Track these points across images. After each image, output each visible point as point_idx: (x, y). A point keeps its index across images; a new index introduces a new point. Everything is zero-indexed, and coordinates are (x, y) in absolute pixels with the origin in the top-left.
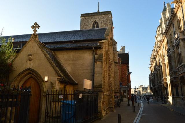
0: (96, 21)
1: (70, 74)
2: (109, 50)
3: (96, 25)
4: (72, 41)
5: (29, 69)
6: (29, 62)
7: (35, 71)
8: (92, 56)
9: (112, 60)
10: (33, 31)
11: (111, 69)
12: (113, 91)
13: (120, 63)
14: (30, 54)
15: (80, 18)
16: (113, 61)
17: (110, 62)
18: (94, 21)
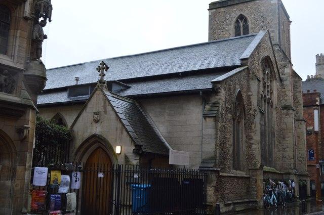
0: (241, 15)
1: (164, 140)
2: (249, 88)
3: (241, 24)
4: (179, 73)
5: (94, 136)
6: (95, 125)
7: (105, 139)
8: (201, 108)
9: (256, 108)
10: (100, 75)
11: (253, 125)
12: (256, 170)
13: (318, 103)
14: (96, 113)
15: (208, 11)
16: (258, 110)
17: (251, 112)
18: (237, 17)
